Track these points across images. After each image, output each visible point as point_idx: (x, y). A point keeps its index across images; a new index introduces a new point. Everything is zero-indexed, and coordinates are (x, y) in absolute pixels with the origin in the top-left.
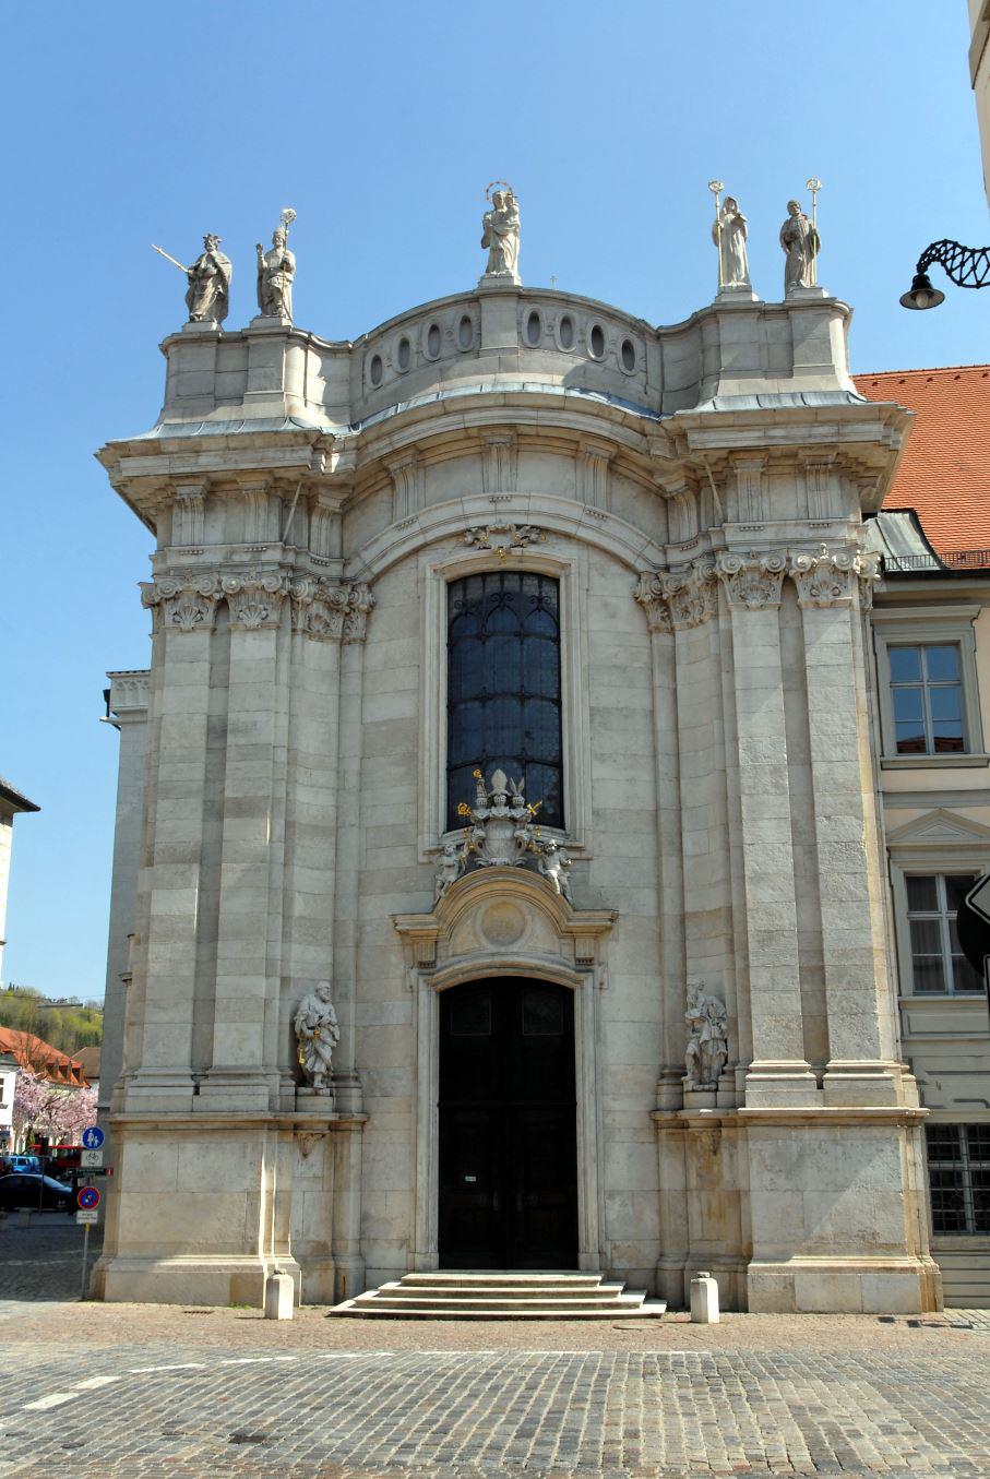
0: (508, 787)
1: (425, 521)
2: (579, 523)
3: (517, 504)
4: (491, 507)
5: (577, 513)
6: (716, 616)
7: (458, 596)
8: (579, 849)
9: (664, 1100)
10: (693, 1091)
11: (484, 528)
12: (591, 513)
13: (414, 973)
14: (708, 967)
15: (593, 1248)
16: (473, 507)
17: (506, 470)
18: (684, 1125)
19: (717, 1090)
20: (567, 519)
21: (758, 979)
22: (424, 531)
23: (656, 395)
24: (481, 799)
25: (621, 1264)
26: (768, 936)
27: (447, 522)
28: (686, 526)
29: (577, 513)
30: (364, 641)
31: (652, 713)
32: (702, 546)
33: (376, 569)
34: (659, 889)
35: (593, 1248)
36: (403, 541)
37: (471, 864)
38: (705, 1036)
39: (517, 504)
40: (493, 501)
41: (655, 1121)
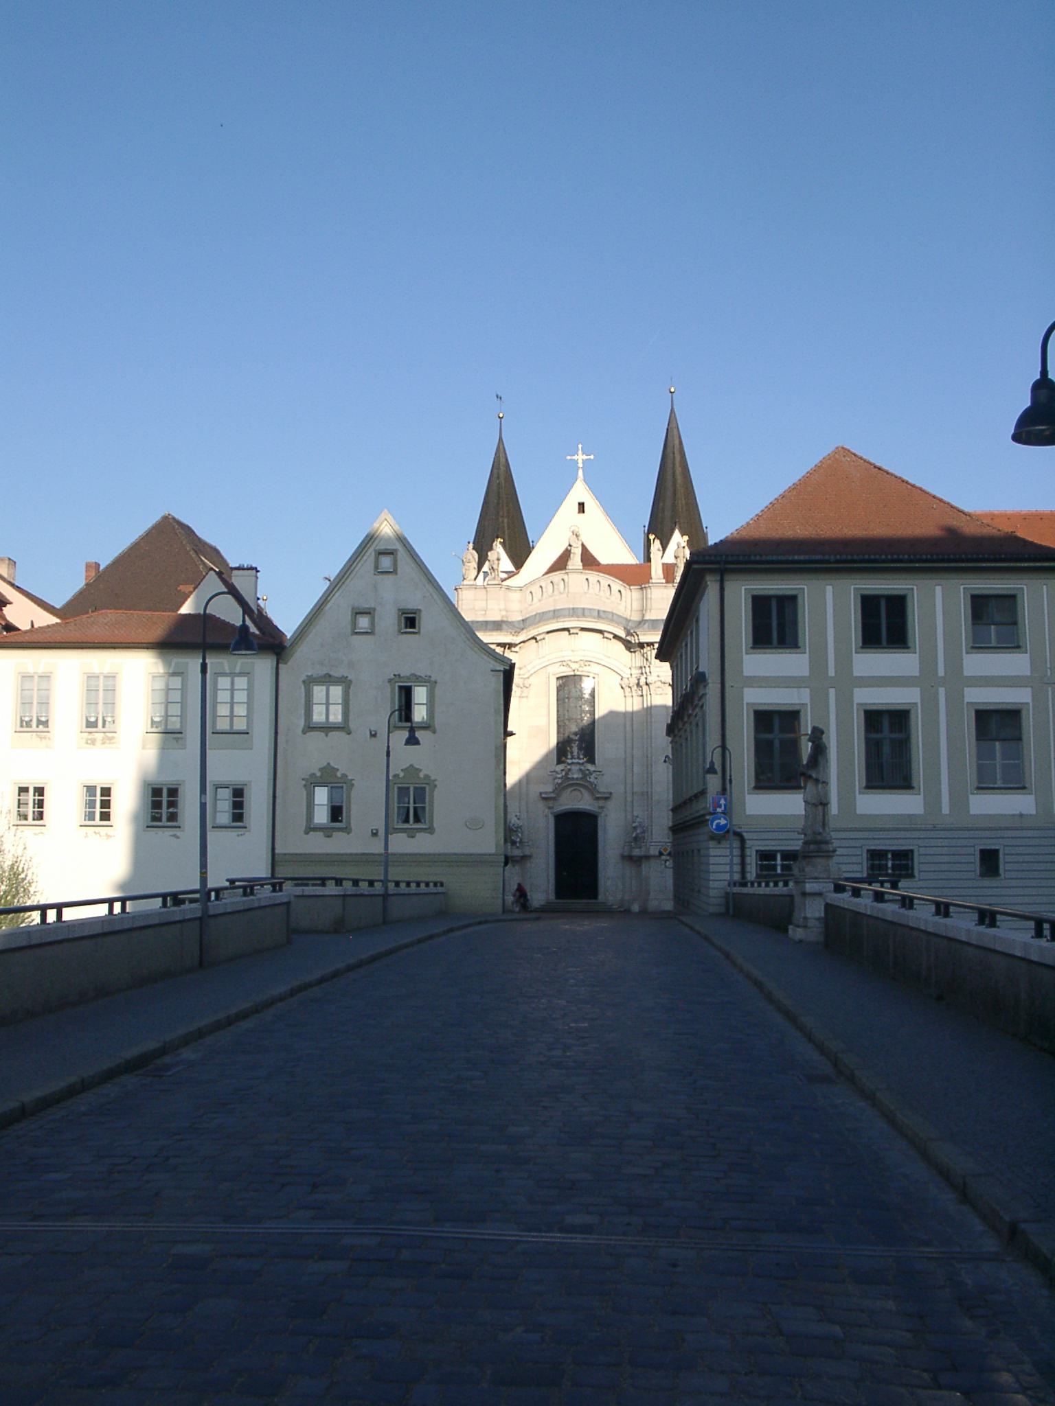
0: (578, 752)
8: (600, 772)
11: (570, 660)
24: (569, 757)
37: (566, 778)
38: (638, 831)
40: (573, 651)
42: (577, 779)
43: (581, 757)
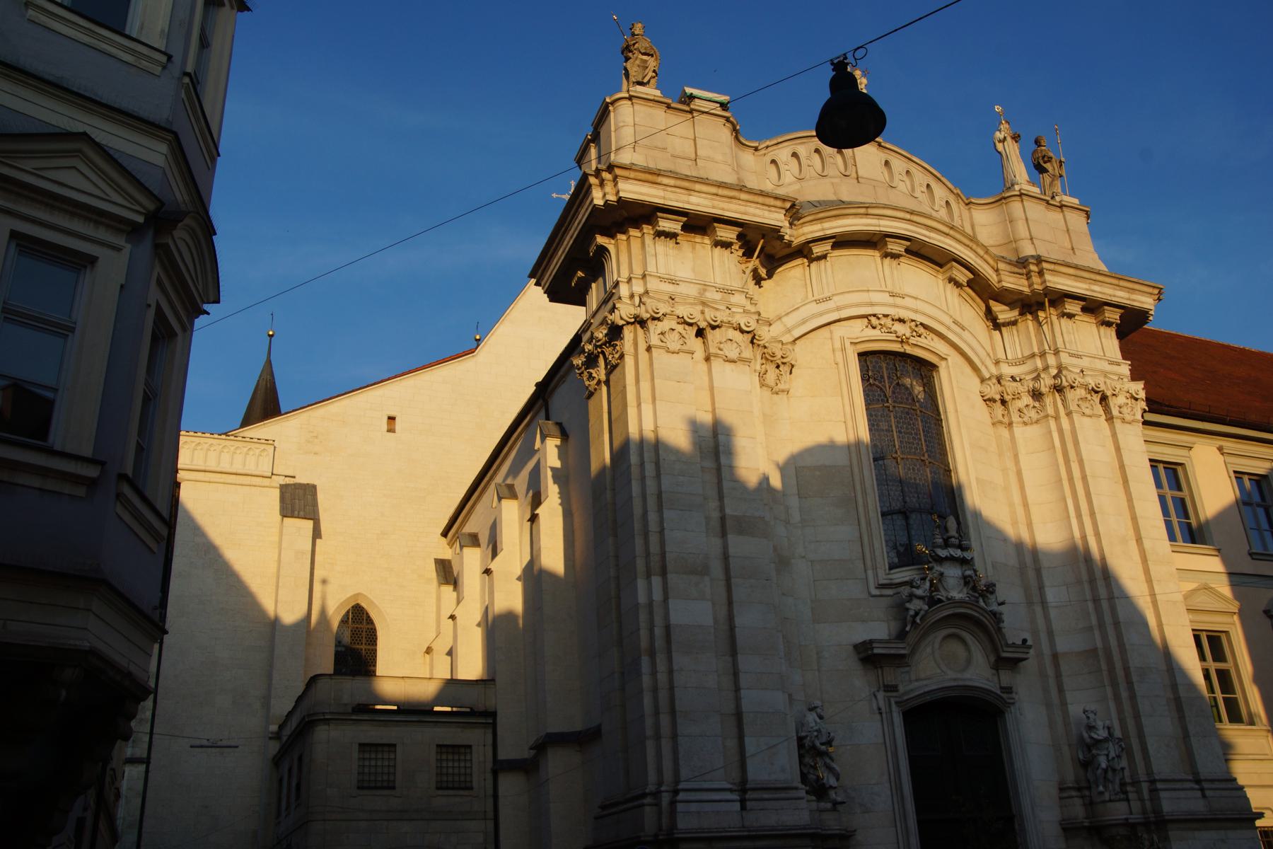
1: (838, 301)
3: (908, 302)
5: (948, 321)
10: (1110, 801)
13: (881, 695)
16: (876, 297)
19: (1128, 800)
22: (838, 309)
27: (857, 305)
29: (948, 321)
36: (821, 314)
39: (908, 302)
42: (961, 603)
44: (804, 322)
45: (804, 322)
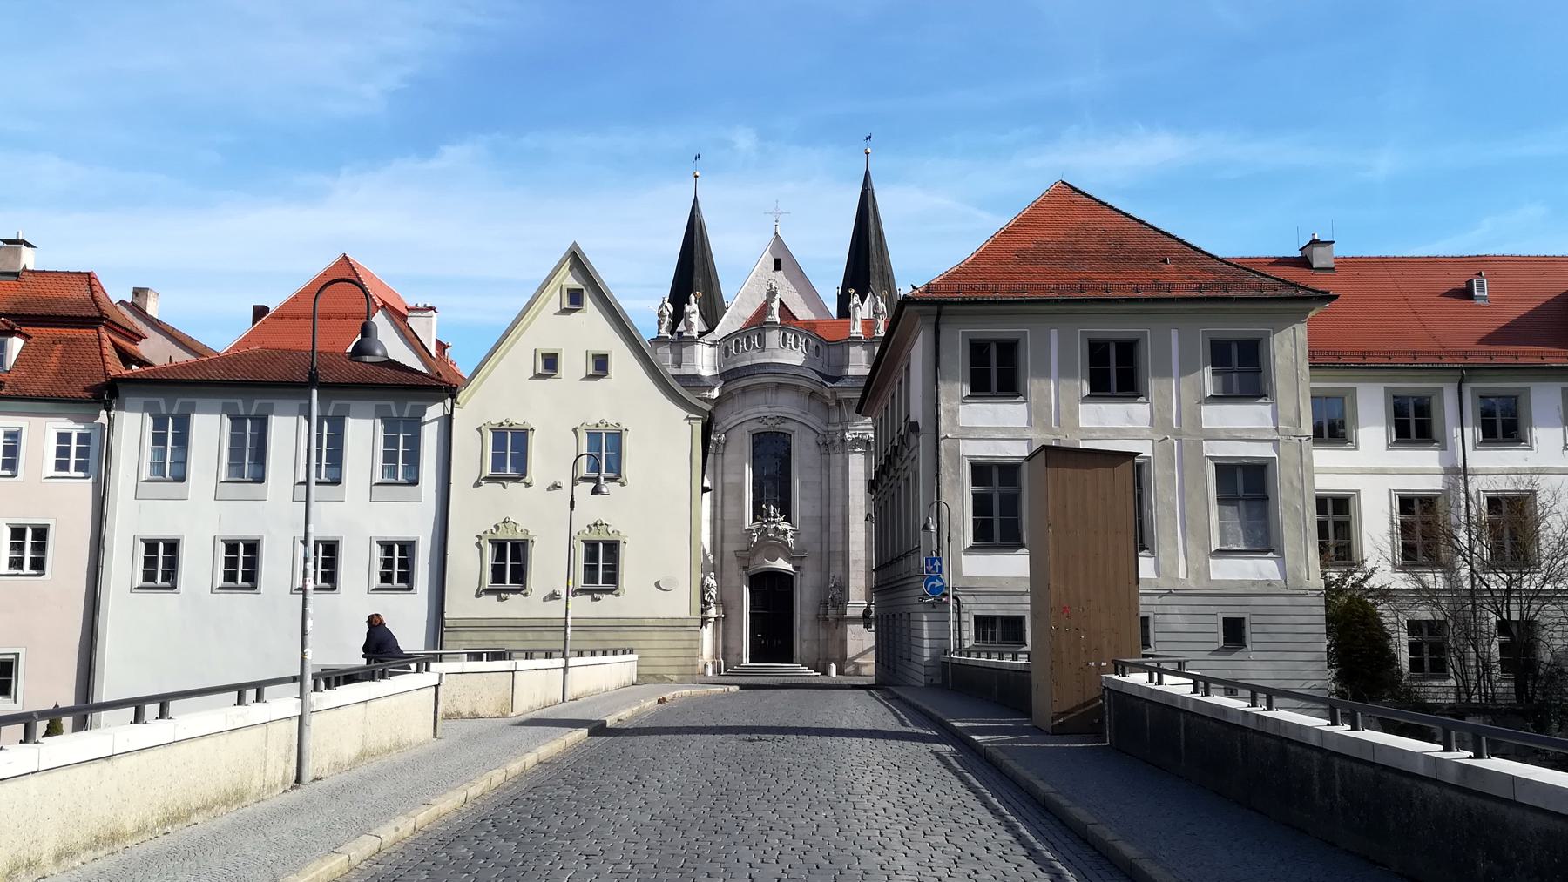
0: (774, 511)
2: (799, 416)
3: (777, 409)
4: (768, 410)
5: (798, 413)
6: (844, 453)
7: (756, 438)
9: (821, 612)
12: (803, 413)
14: (837, 571)
15: (798, 656)
16: (761, 409)
17: (773, 395)
18: (828, 619)
20: (794, 415)
21: (852, 575)
22: (745, 416)
23: (826, 367)
25: (806, 662)
26: (856, 562)
28: (836, 418)
29: (798, 413)
30: (723, 454)
31: (821, 483)
32: (839, 427)
33: (727, 428)
34: (822, 543)
35: (798, 656)
39: (777, 409)
41: (818, 618)
43: (778, 515)
44: (729, 424)
45: (729, 424)
